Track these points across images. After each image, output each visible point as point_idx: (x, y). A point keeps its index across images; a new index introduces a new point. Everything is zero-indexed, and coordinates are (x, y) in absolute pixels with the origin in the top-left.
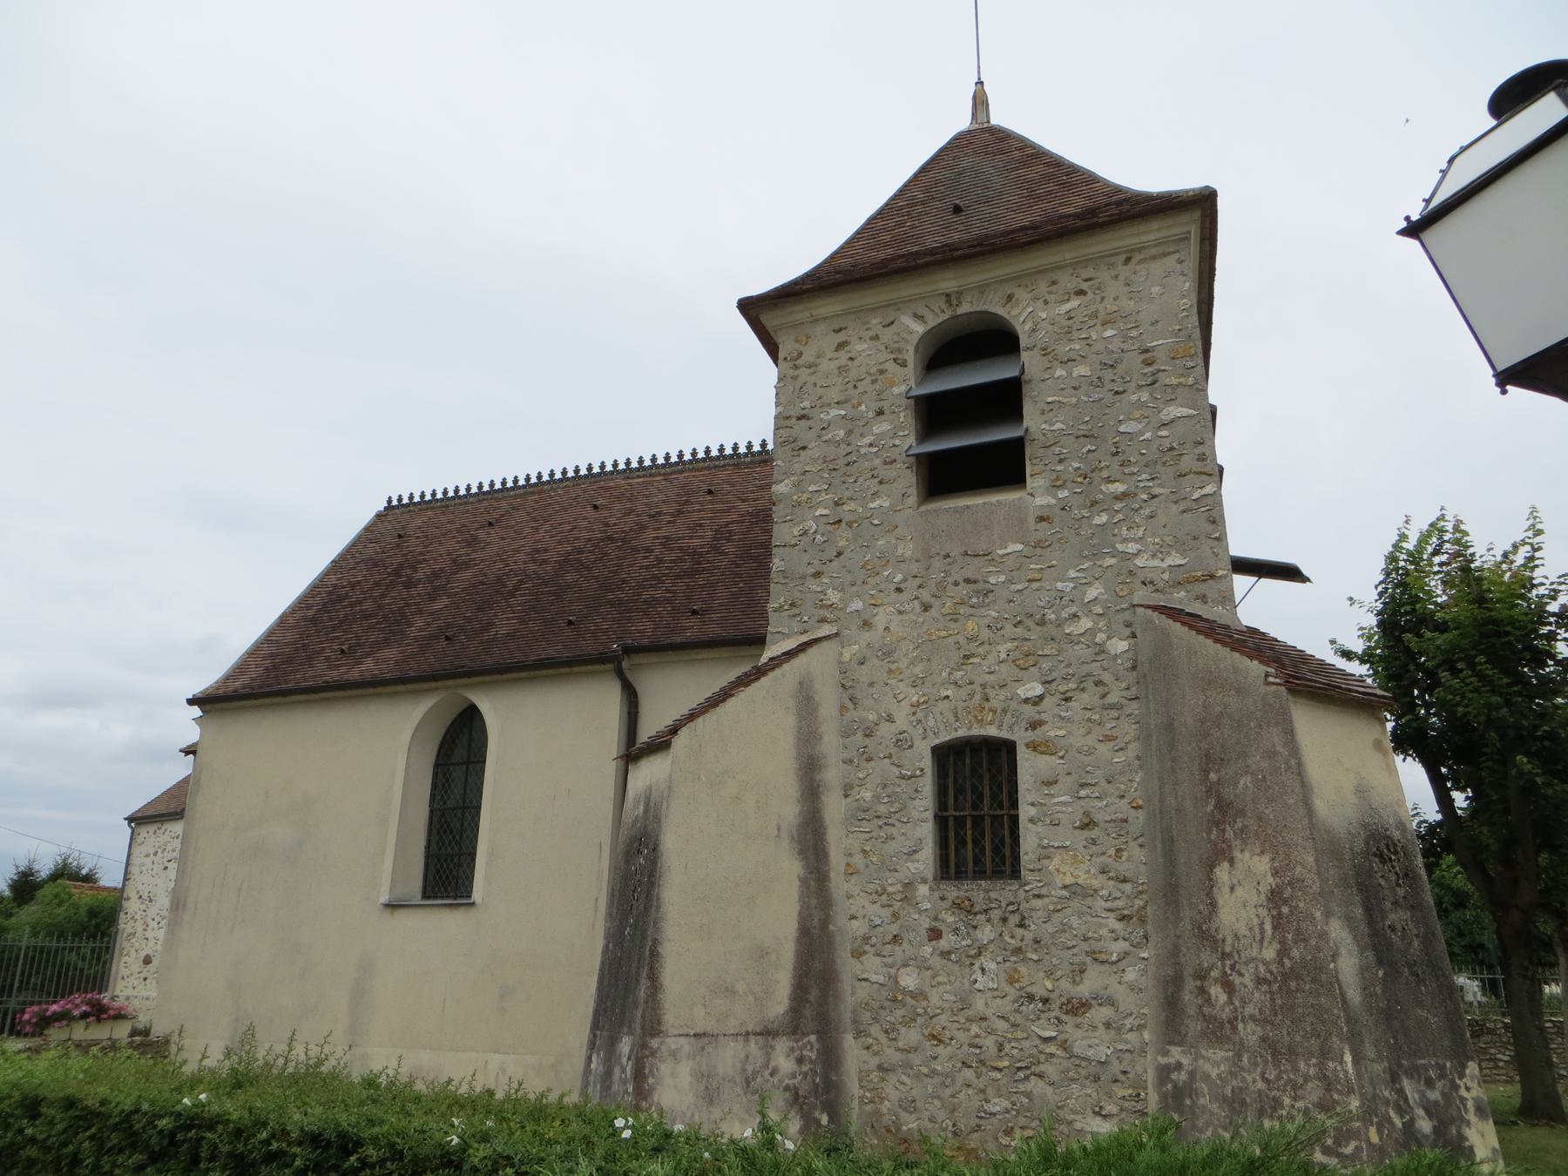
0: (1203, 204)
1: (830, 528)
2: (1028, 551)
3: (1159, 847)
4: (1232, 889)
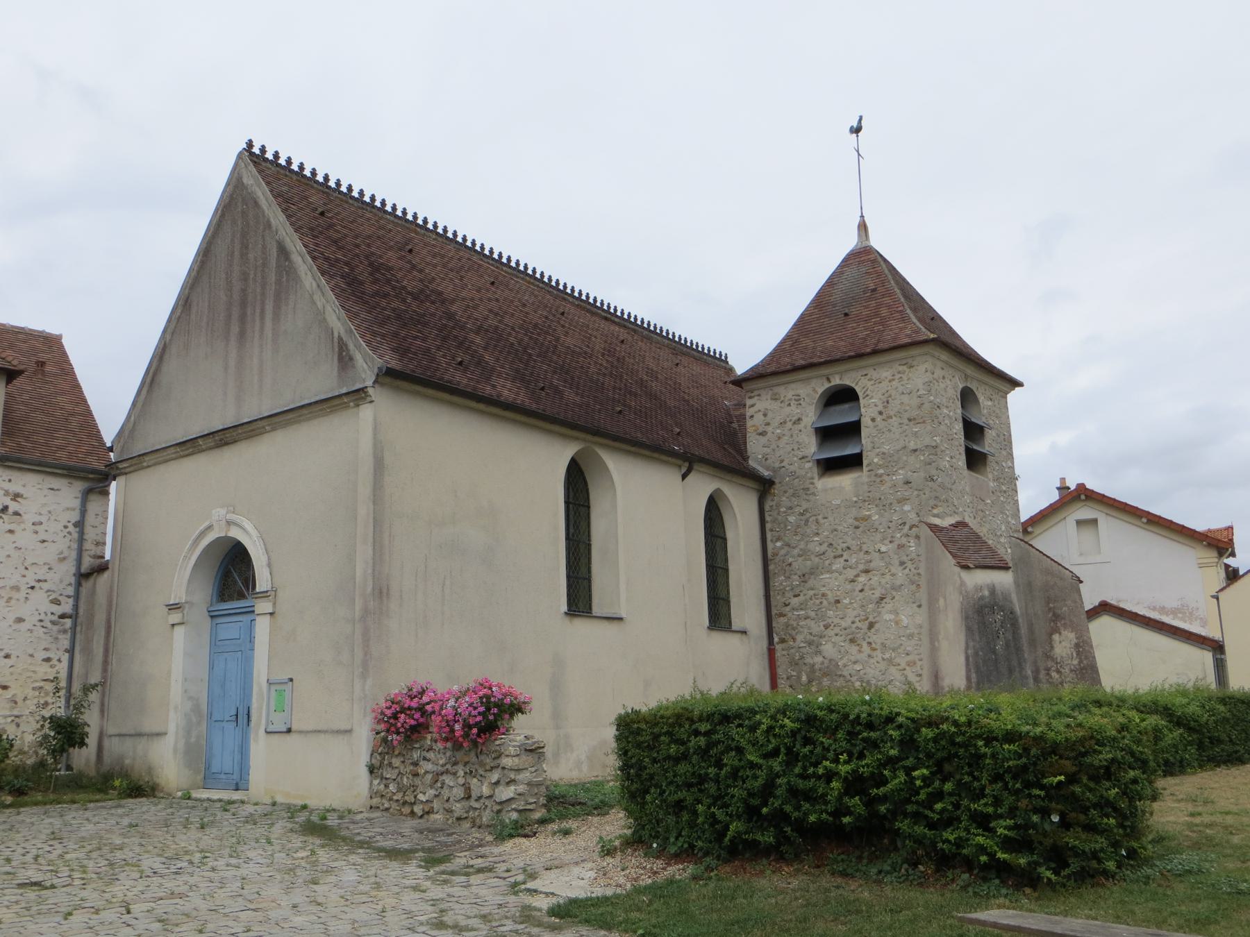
4: (1060, 642)
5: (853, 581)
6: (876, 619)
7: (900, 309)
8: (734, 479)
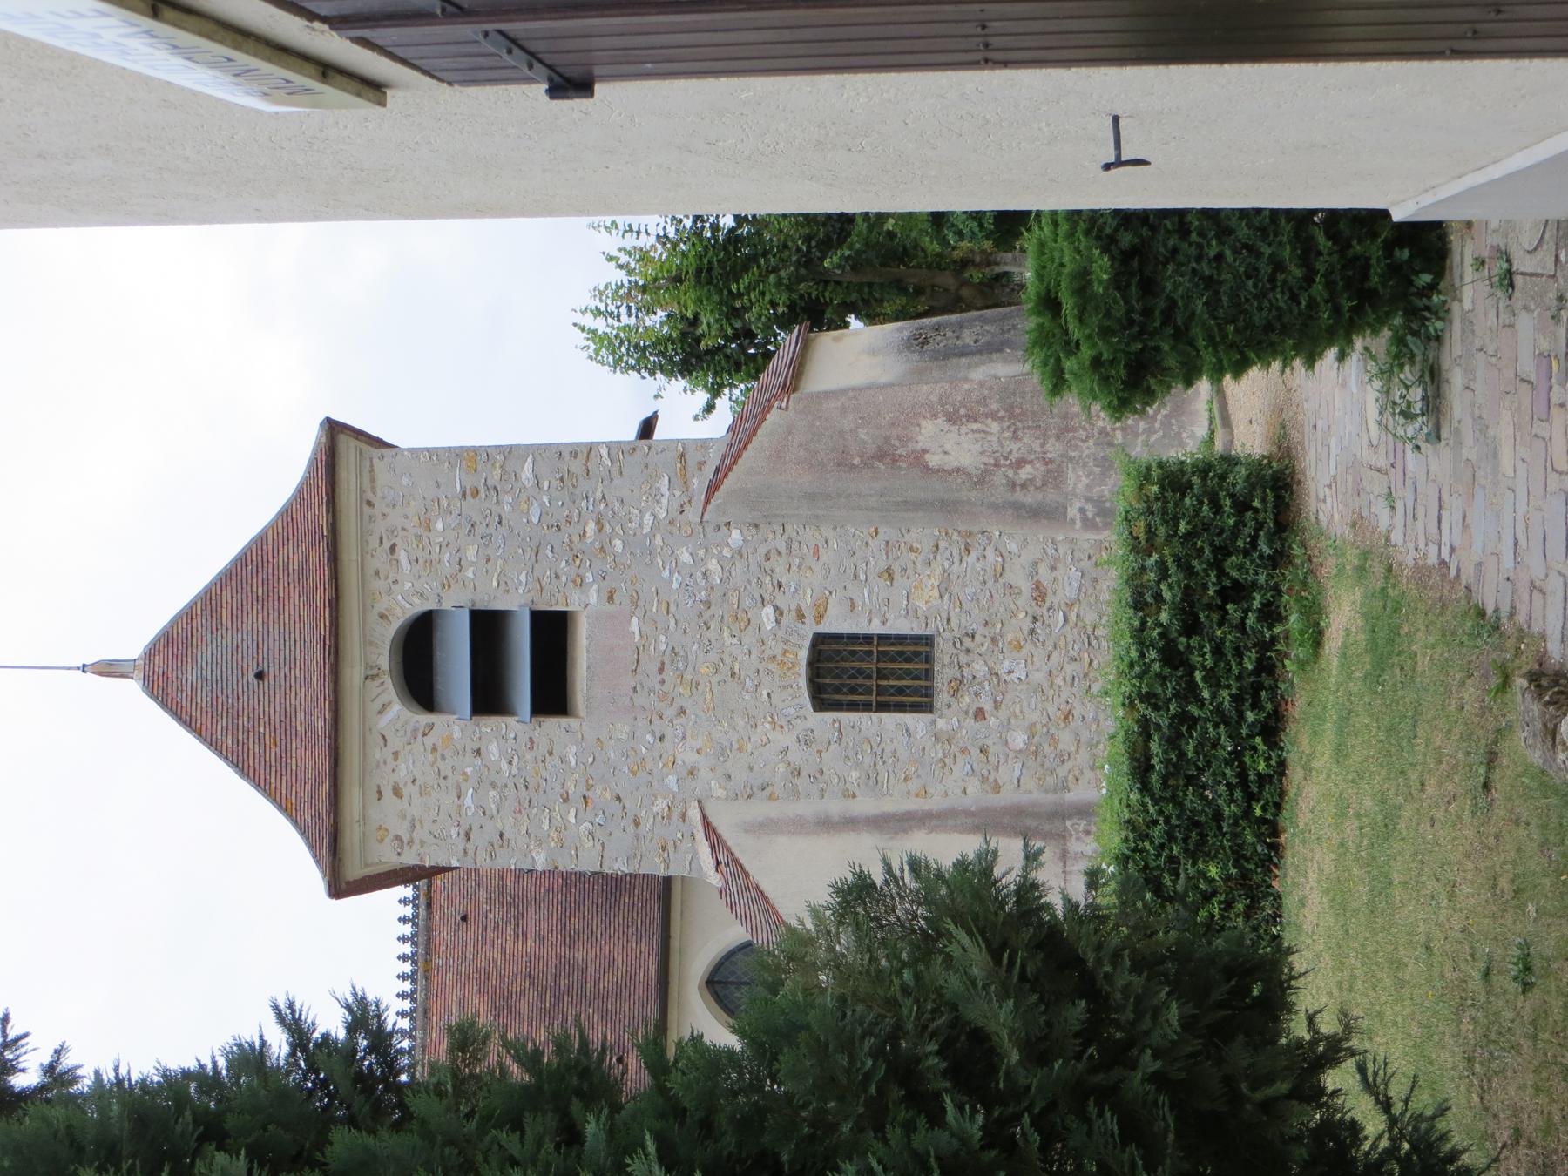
0: (333, 430)
1: (590, 807)
2: (640, 612)
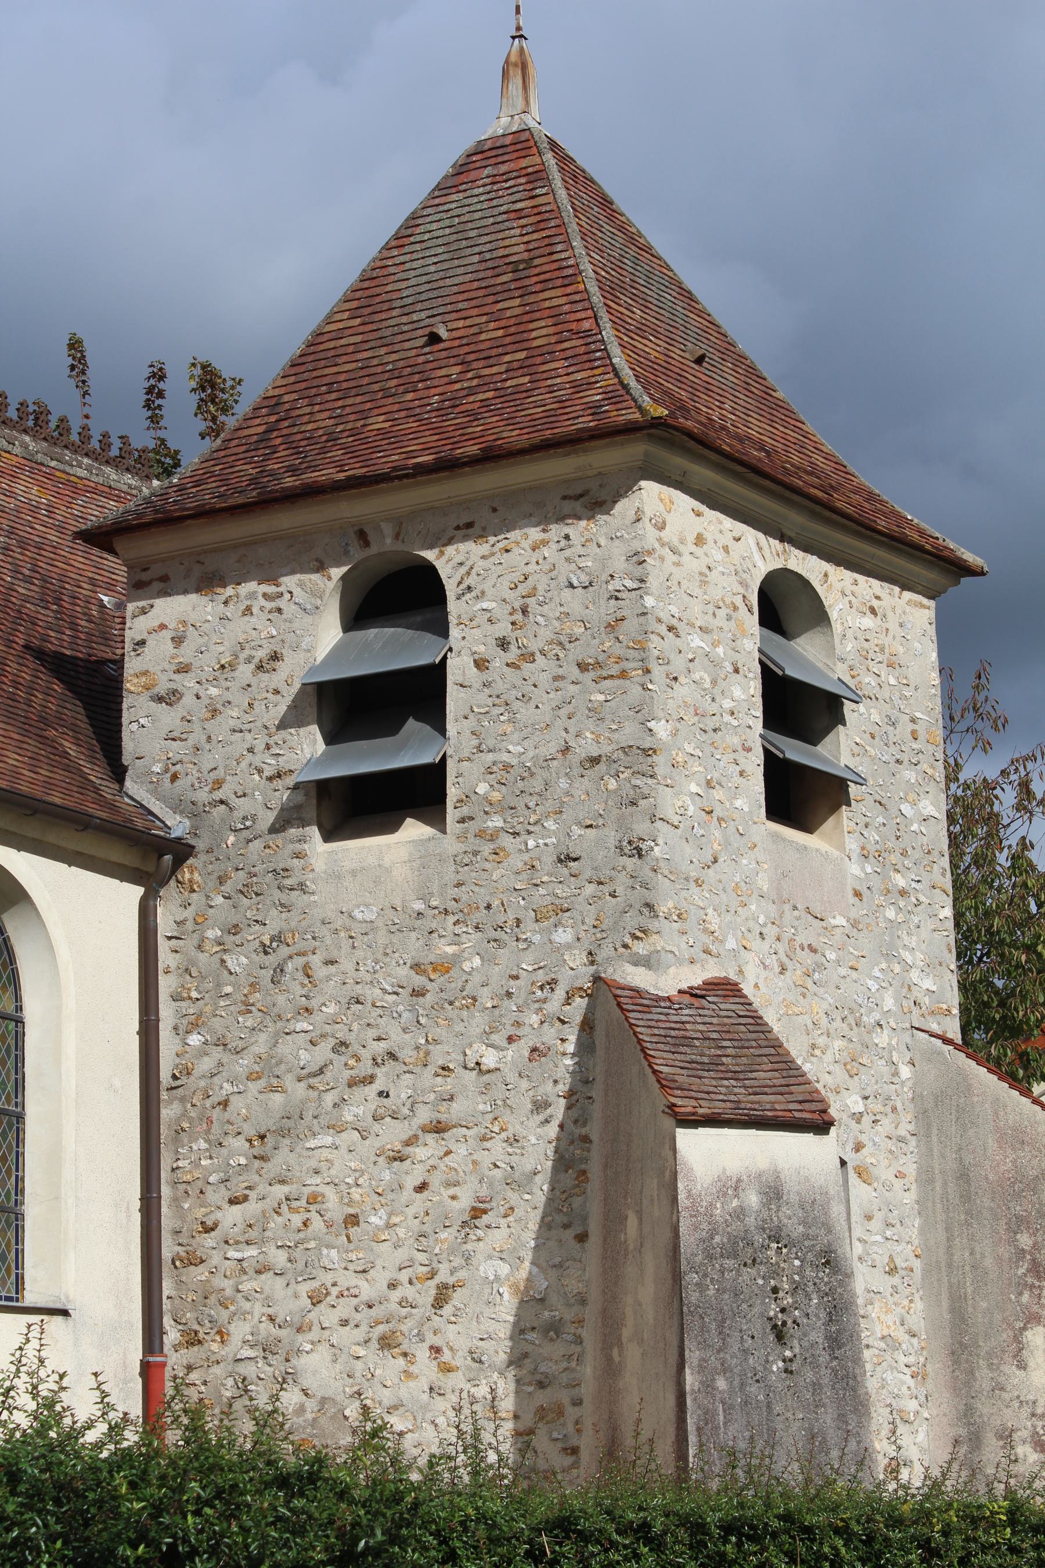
3: (945, 1304)
5: (399, 1158)
6: (462, 1274)
7: (586, 325)
8: (52, 837)
